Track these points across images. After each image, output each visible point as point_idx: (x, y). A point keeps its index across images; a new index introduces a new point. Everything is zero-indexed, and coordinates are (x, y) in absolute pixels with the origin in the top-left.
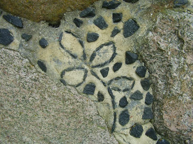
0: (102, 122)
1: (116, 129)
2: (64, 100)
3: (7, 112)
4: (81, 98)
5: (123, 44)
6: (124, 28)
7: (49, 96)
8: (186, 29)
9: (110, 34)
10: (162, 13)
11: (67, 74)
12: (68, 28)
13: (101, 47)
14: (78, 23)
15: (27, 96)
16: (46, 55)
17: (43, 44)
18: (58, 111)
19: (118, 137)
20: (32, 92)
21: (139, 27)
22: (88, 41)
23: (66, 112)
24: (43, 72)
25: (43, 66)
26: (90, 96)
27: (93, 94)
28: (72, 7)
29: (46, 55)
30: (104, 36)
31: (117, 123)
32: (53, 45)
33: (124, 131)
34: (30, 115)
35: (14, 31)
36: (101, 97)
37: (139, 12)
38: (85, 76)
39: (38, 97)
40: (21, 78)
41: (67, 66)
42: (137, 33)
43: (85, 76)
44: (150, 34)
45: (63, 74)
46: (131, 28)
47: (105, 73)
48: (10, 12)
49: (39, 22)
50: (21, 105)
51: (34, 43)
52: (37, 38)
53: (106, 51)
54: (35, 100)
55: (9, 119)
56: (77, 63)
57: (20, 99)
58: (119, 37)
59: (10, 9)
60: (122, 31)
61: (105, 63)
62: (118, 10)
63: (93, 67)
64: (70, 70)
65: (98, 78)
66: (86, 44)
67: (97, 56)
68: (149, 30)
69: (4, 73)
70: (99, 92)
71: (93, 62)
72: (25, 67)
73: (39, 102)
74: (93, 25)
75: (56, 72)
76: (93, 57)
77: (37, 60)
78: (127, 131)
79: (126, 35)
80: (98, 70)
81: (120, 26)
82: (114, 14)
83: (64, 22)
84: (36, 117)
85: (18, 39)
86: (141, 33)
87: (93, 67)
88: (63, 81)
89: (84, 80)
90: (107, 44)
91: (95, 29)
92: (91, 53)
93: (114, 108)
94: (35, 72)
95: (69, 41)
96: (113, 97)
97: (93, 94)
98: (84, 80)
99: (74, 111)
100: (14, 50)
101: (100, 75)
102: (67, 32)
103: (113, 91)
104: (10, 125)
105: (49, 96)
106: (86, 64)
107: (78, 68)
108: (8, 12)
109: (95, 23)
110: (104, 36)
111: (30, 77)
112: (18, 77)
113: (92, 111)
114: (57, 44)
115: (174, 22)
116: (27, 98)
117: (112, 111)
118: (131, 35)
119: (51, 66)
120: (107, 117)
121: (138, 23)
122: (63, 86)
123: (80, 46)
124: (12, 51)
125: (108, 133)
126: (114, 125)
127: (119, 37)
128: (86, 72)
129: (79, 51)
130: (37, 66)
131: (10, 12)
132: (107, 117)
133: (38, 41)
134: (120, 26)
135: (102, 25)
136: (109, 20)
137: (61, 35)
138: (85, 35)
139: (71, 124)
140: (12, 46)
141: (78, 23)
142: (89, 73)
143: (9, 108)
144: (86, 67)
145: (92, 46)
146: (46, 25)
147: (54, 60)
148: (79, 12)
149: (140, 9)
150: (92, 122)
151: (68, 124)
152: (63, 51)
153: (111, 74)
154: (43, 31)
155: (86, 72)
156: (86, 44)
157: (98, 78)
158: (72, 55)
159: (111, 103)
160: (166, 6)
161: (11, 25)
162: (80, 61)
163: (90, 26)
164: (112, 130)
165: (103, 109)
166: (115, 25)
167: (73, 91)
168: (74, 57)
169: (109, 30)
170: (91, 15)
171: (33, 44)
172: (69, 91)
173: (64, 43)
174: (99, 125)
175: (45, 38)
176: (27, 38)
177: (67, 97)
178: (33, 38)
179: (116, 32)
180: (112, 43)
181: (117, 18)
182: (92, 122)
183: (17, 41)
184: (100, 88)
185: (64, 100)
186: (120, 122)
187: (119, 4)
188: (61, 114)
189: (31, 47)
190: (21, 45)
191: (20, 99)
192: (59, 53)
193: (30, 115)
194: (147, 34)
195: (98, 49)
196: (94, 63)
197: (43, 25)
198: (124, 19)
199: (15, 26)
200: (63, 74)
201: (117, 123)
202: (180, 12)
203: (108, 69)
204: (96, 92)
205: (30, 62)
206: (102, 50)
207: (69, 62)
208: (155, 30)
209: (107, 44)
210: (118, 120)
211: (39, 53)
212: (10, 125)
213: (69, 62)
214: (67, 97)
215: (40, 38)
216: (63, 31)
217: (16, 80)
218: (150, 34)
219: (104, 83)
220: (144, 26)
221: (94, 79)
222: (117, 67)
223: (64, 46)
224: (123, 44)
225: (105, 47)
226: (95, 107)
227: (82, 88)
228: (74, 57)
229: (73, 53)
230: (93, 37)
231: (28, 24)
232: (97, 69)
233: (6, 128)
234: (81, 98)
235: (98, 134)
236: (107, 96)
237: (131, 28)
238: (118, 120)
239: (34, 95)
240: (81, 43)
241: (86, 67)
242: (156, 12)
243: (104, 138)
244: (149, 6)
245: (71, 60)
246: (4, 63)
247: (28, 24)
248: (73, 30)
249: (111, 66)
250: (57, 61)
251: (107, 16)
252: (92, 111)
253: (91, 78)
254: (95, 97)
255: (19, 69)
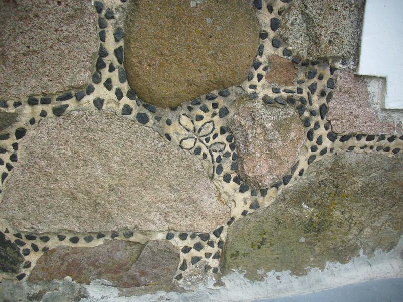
0: (205, 173)
1: (215, 177)
2: (183, 159)
3: (145, 169)
4: (192, 157)
5: (219, 122)
6: (219, 112)
7: (173, 157)
8: (257, 113)
9: (211, 116)
10: (243, 104)
11: (184, 142)
12: (184, 112)
13: (205, 124)
14: (190, 109)
15: (159, 157)
16: (170, 130)
17: (169, 123)
18: (178, 166)
19: (215, 182)
20: (162, 154)
21: (229, 112)
22: (197, 121)
23: (184, 167)
24: (168, 141)
25: (168, 137)
26: (198, 156)
27: (200, 154)
28: (187, 99)
29: (170, 130)
30: (207, 117)
31: (215, 173)
32: (175, 123)
33: (219, 178)
34: (161, 170)
35: (149, 114)
36: (205, 156)
37: (229, 103)
38: (195, 143)
39: (165, 157)
40: (155, 145)
41: (184, 137)
42: (228, 116)
43: (195, 143)
44: (236, 116)
45: (181, 142)
46: (224, 113)
47: (207, 140)
48: (147, 102)
49: (165, 108)
50: (154, 163)
51: (163, 123)
52: (164, 119)
53: (208, 127)
54: (164, 159)
55: (146, 173)
56: (190, 135)
57: (154, 159)
58: (216, 118)
59: (148, 100)
60: (218, 114)
61: (208, 134)
62: (216, 101)
63: (201, 137)
64: (186, 139)
65: (203, 144)
66: (196, 122)
67: (203, 130)
68: (235, 114)
69: (143, 143)
70: (204, 153)
71: (200, 133)
72: (157, 138)
73: (166, 161)
74: (200, 110)
75: (177, 141)
76: (200, 130)
77: (165, 133)
78: (221, 179)
79: (221, 116)
80: (203, 139)
81: (217, 111)
82: (213, 104)
83: (181, 108)
84: (165, 171)
85: (152, 119)
86: (230, 116)
87: (201, 137)
88: (181, 147)
89: (195, 145)
90: (209, 122)
91: (201, 113)
92: (199, 128)
93: (213, 163)
94: (164, 142)
95: (185, 120)
96: (212, 156)
97: (200, 154)
98: (195, 145)
99: (189, 166)
100: (149, 127)
101: (204, 142)
102: (184, 115)
103: (212, 152)
104: (147, 178)
105: (173, 157)
106: (195, 135)
107: (191, 138)
108: (145, 102)
109: (201, 108)
110: (207, 117)
111: (161, 144)
112: (153, 144)
113: (199, 165)
114: (177, 123)
115: (250, 109)
116: (158, 158)
117: (212, 165)
118: (224, 116)
119: (174, 137)
120: (209, 169)
121: (228, 110)
122: (181, 150)
123: (192, 124)
124: (148, 128)
125: (209, 180)
126: (213, 174)
127: (216, 118)
128: (196, 139)
129: (191, 127)
130: (164, 137)
131: (147, 102)
132: (209, 169)
133: (165, 121)
134: (217, 111)
135: (205, 110)
136: (210, 107)
137: (180, 117)
138: (195, 117)
139: (187, 174)
140: (148, 124)
141: (190, 109)
142: (198, 140)
143: (146, 166)
144: (196, 137)
145: (199, 124)
146: (169, 110)
147: (175, 133)
148: (190, 101)
149: (229, 101)
150: (199, 173)
151: (185, 175)
152: (181, 127)
153: (212, 141)
154: (168, 114)
155: (196, 139)
156: (196, 122)
157: (203, 144)
158: (186, 129)
159: (211, 160)
160: (245, 99)
161: (147, 110)
162: (192, 133)
163: (198, 111)
164: (212, 178)
165: (206, 164)
166: (213, 110)
167: (188, 153)
168: (188, 130)
169: (210, 113)
170: (199, 103)
171: (162, 123)
172: (185, 153)
173: (182, 122)
174: (203, 175)
175: (170, 119)
176: (158, 119)
177: (184, 157)
178: (162, 119)
179: (214, 115)
180: (212, 121)
181: (215, 106)
182: (199, 173)
183: (151, 121)
184: (205, 150)
185: (183, 159)
186: (217, 172)
187: (216, 97)
188: (181, 168)
189: (161, 125)
190: (154, 123)
191: (154, 159)
192: (179, 128)
193: (161, 170)
194: (234, 116)
195: (203, 126)
196: (201, 134)
197: (168, 110)
198: (220, 107)
199: (150, 111)
200: (181, 142)
201: (215, 173)
202: (253, 103)
203: (209, 138)
204: (202, 153)
205: (160, 135)
206: (205, 126)
207: (185, 134)
208: (238, 114)
209: (209, 122)
210: (215, 171)
211: (167, 129)
212: (147, 178)
213: (185, 134)
214: (184, 157)
215: (167, 118)
216: (181, 114)
217: (152, 147)
218: (236, 116)
219: (207, 147)
220: (232, 112)
221: (201, 144)
222: (215, 136)
223: (182, 124)
224: (219, 122)
225: (207, 124)
226: (201, 163)
227: (193, 150)
228: (188, 130)
229: (187, 128)
230: (200, 118)
231: (159, 110)
232: (202, 138)
233: (143, 180)
234: (192, 157)
235: (203, 181)
236: (209, 155)
237: (224, 113)
238: (215, 171)
239: (163, 156)
240: (193, 122)
241: (196, 137)
242: (239, 103)
243: (207, 184)
244: (235, 99)
245: (187, 133)
246: (143, 135)
247: (159, 110)
248: (187, 113)
249: (211, 136)
250: (178, 134)
251: (209, 104)
252: (199, 165)
253: (199, 144)
254: (201, 156)
255: (154, 139)
